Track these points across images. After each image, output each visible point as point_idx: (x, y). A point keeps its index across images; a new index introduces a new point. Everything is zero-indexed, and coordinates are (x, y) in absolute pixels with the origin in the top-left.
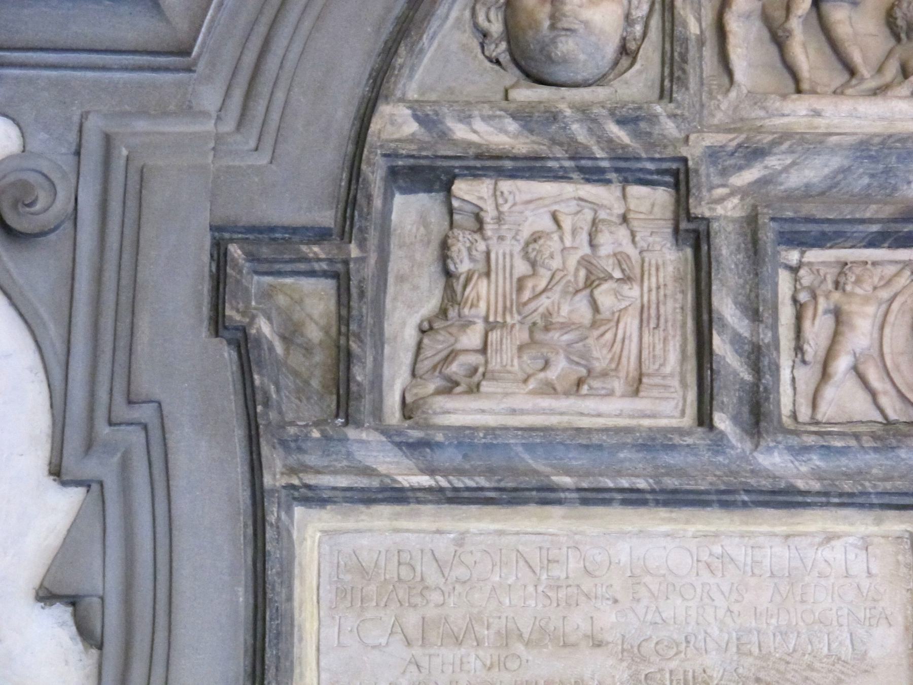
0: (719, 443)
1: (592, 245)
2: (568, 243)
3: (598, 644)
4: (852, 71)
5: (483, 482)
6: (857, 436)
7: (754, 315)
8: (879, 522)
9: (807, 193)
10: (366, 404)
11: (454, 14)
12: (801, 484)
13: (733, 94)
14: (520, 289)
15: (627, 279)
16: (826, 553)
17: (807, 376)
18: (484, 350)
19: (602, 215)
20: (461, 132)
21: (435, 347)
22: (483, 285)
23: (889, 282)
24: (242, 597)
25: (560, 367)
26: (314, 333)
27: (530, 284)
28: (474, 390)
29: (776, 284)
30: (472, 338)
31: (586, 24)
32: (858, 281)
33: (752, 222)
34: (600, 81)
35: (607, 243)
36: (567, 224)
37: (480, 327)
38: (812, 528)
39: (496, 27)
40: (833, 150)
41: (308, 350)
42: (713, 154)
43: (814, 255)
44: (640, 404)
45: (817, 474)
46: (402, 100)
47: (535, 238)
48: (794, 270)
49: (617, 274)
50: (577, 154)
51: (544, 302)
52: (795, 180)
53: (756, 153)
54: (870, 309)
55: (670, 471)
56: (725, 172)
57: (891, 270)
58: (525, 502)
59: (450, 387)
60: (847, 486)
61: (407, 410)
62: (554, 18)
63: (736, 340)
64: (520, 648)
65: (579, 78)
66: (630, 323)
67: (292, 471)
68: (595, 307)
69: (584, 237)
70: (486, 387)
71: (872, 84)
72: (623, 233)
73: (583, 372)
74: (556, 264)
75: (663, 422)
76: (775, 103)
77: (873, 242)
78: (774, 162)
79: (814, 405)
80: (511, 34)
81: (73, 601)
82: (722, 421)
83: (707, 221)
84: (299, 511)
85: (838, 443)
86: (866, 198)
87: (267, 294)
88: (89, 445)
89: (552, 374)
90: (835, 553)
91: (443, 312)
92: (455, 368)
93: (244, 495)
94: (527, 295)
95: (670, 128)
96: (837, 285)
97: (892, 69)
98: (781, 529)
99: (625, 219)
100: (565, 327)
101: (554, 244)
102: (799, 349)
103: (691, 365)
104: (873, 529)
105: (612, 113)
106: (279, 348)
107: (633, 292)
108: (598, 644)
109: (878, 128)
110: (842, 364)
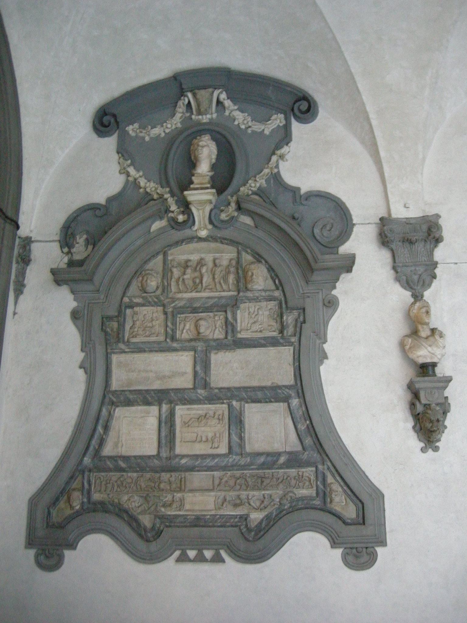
0: (167, 343)
1: (152, 315)
2: (149, 315)
3: (152, 371)
4: (188, 289)
5: (136, 350)
6: (186, 341)
7: (172, 324)
8: (189, 353)
9: (181, 307)
10: (121, 340)
11: (135, 283)
12: (178, 348)
13: (172, 293)
14: (143, 322)
15: (157, 320)
16: (181, 357)
17: (180, 333)
18: (138, 331)
19: (154, 311)
20: (135, 301)
21: (132, 331)
22: (138, 322)
23: (192, 319)
24: (104, 367)
25: (148, 333)
26: (115, 330)
27: (144, 322)
28: (136, 337)
29: (177, 320)
30: (136, 330)
31: (151, 285)
32: (188, 319)
33: (173, 312)
34: (154, 292)
35: (154, 315)
36: (149, 313)
37: (137, 328)
38: (180, 354)
39: (140, 285)
40: (185, 300)
41: (114, 332)
42: (169, 302)
43: (182, 316)
44: (157, 338)
45: (181, 347)
46: (127, 297)
47: (145, 315)
48: (179, 317)
49: (156, 319)
50: (149, 302)
51: (146, 324)
52: (179, 305)
53: (174, 302)
54: (189, 323)
55: (161, 347)
56: (170, 305)
57: (192, 317)
58: (142, 352)
59: (133, 337)
60: (184, 348)
61: (128, 339)
62: (146, 284)
63: (170, 328)
64: (141, 372)
65: (150, 292)
66: (157, 326)
67: (111, 349)
68: (153, 325)
69: (151, 314)
70: (138, 336)
71: (190, 291)
72: (157, 314)
73: (150, 333)
74: (148, 318)
75: (161, 340)
76: (177, 294)
77: (190, 313)
78: (177, 302)
79: (181, 336)
80: (142, 286)
81: (84, 368)
82: (168, 340)
83: (167, 312)
84: (113, 355)
85: (183, 342)
86: (188, 307)
87: (109, 324)
88: (86, 346)
89: (147, 334)
90: (183, 357)
91: (132, 326)
92: (134, 334)
93: (105, 353)
94: (144, 323)
95: (162, 298)
96: (185, 320)
97: (193, 289)
98: (176, 354)
99: (157, 311)
100: (148, 327)
101: (147, 316)
102: (179, 329)
103: (165, 332)
104: (188, 354)
105: (155, 297)
106: (110, 332)
107: (157, 322)
108: (152, 371)
109: (191, 297)
110: (185, 331)
